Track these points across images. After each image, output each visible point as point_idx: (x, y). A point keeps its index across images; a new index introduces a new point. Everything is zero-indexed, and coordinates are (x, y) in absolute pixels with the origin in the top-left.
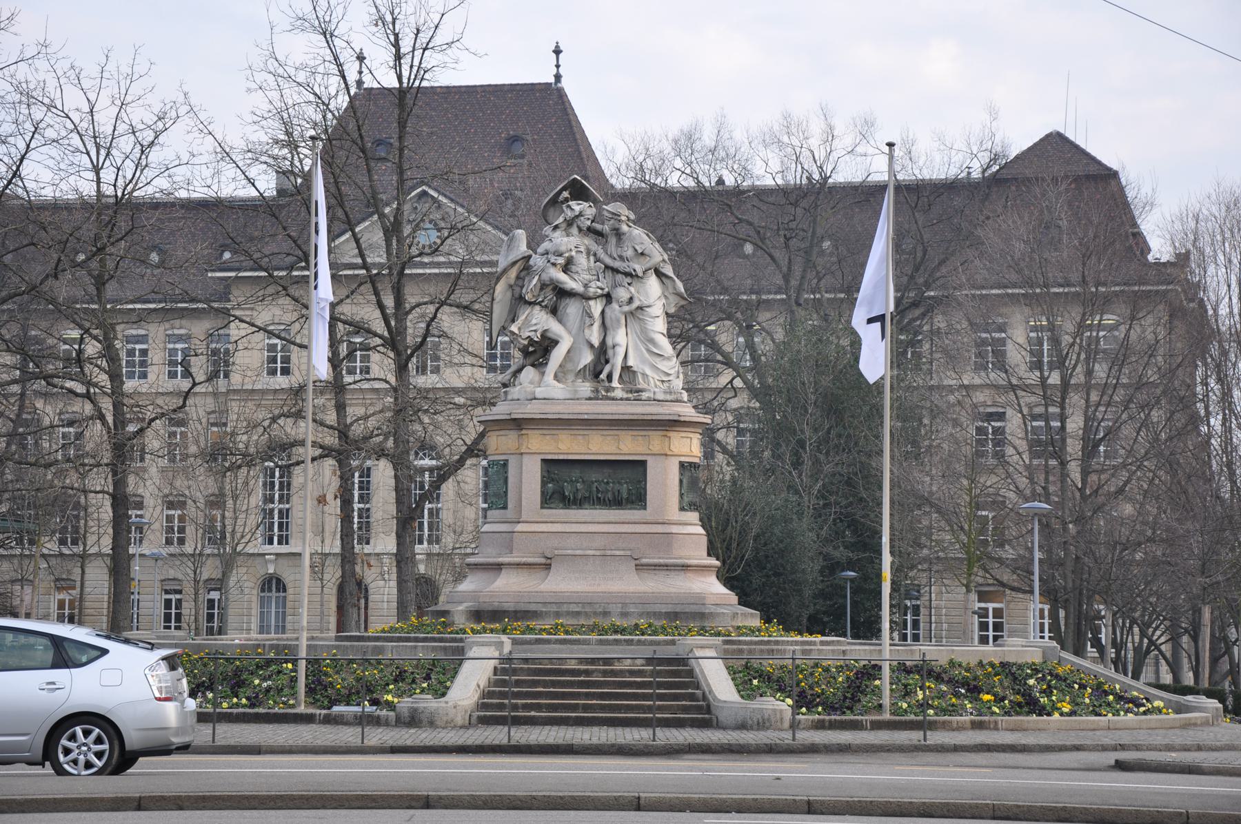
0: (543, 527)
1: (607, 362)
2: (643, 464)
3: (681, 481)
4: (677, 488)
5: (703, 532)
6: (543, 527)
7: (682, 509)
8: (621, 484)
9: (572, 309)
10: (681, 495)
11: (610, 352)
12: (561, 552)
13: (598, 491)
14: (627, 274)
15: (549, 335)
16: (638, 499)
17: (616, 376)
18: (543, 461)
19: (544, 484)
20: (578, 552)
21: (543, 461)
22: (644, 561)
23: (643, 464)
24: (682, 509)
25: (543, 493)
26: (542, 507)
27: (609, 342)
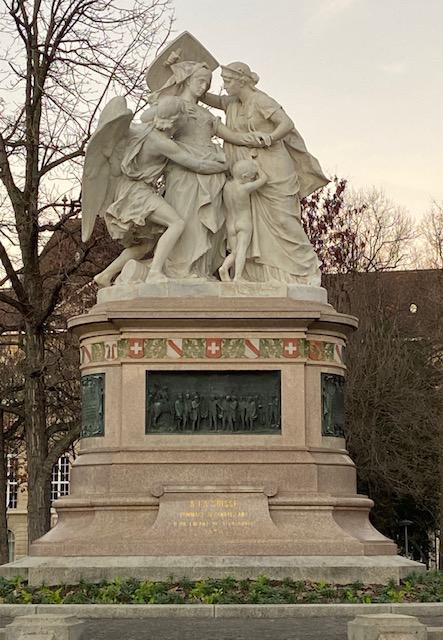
0: (150, 458)
1: (228, 253)
2: (277, 373)
3: (323, 397)
4: (320, 407)
5: (350, 462)
6: (150, 458)
7: (325, 434)
8: (247, 402)
9: (183, 186)
10: (325, 416)
11: (232, 240)
12: (171, 488)
13: (218, 410)
14: (251, 146)
15: (155, 218)
16: (268, 419)
17: (238, 269)
18: (149, 373)
19: (151, 400)
20: (194, 488)
21: (149, 373)
22: (280, 500)
23: (277, 373)
24: (325, 434)
25: (148, 412)
26: (147, 432)
27: (231, 228)
